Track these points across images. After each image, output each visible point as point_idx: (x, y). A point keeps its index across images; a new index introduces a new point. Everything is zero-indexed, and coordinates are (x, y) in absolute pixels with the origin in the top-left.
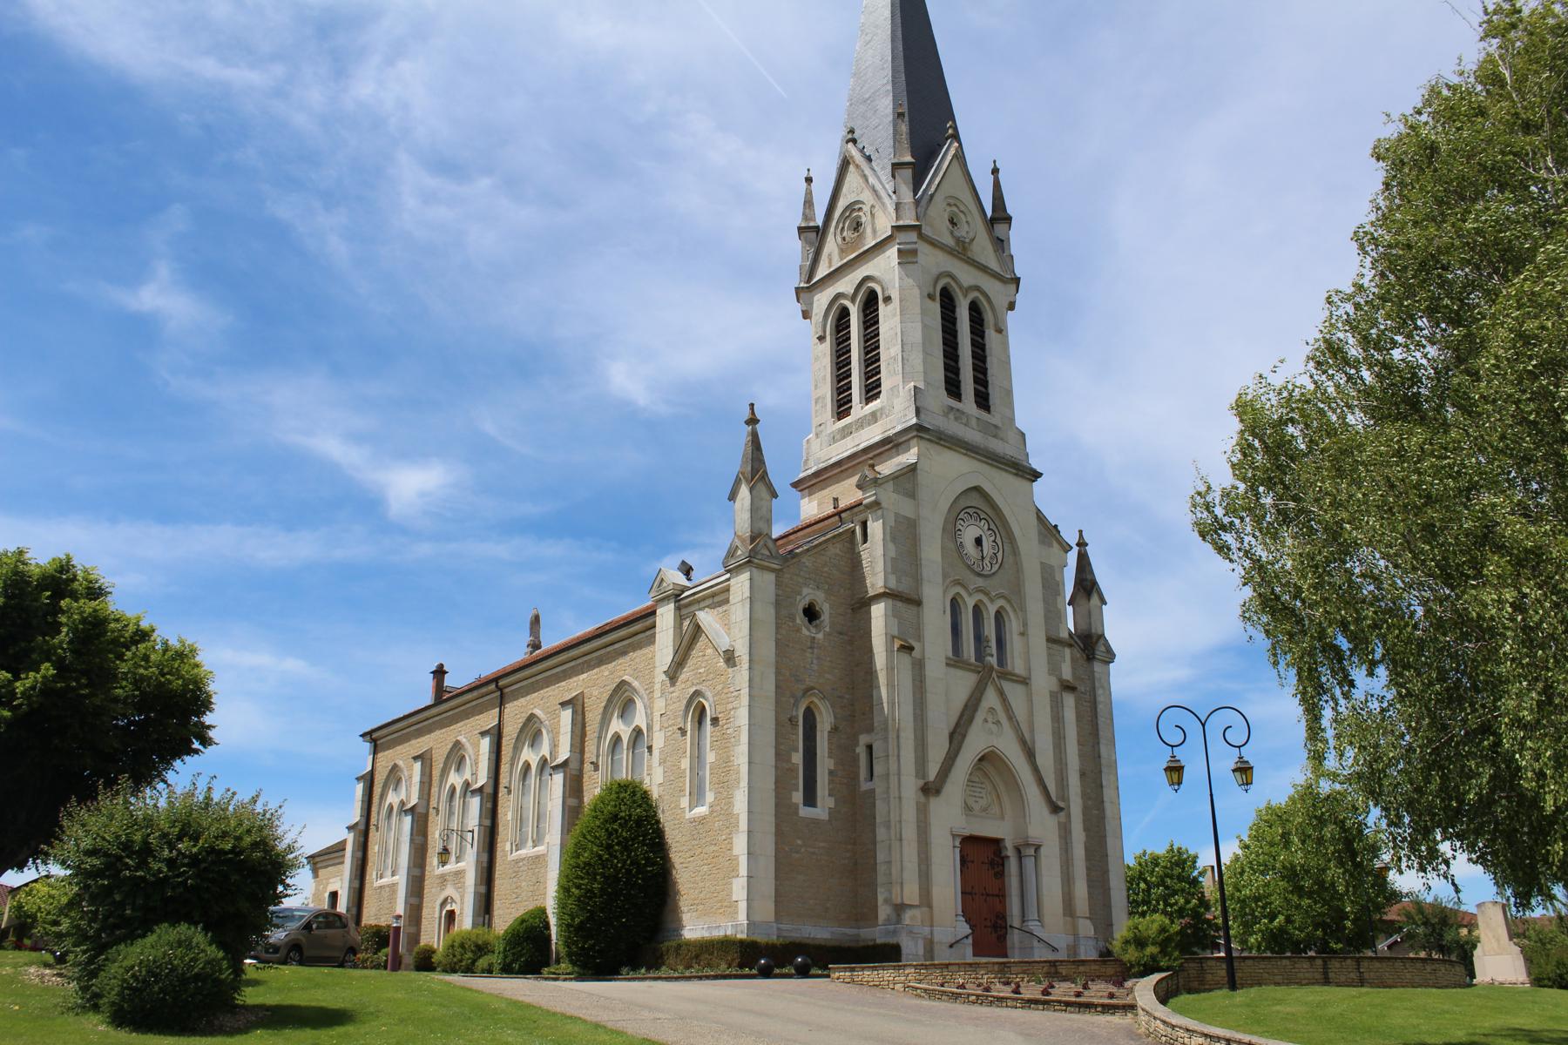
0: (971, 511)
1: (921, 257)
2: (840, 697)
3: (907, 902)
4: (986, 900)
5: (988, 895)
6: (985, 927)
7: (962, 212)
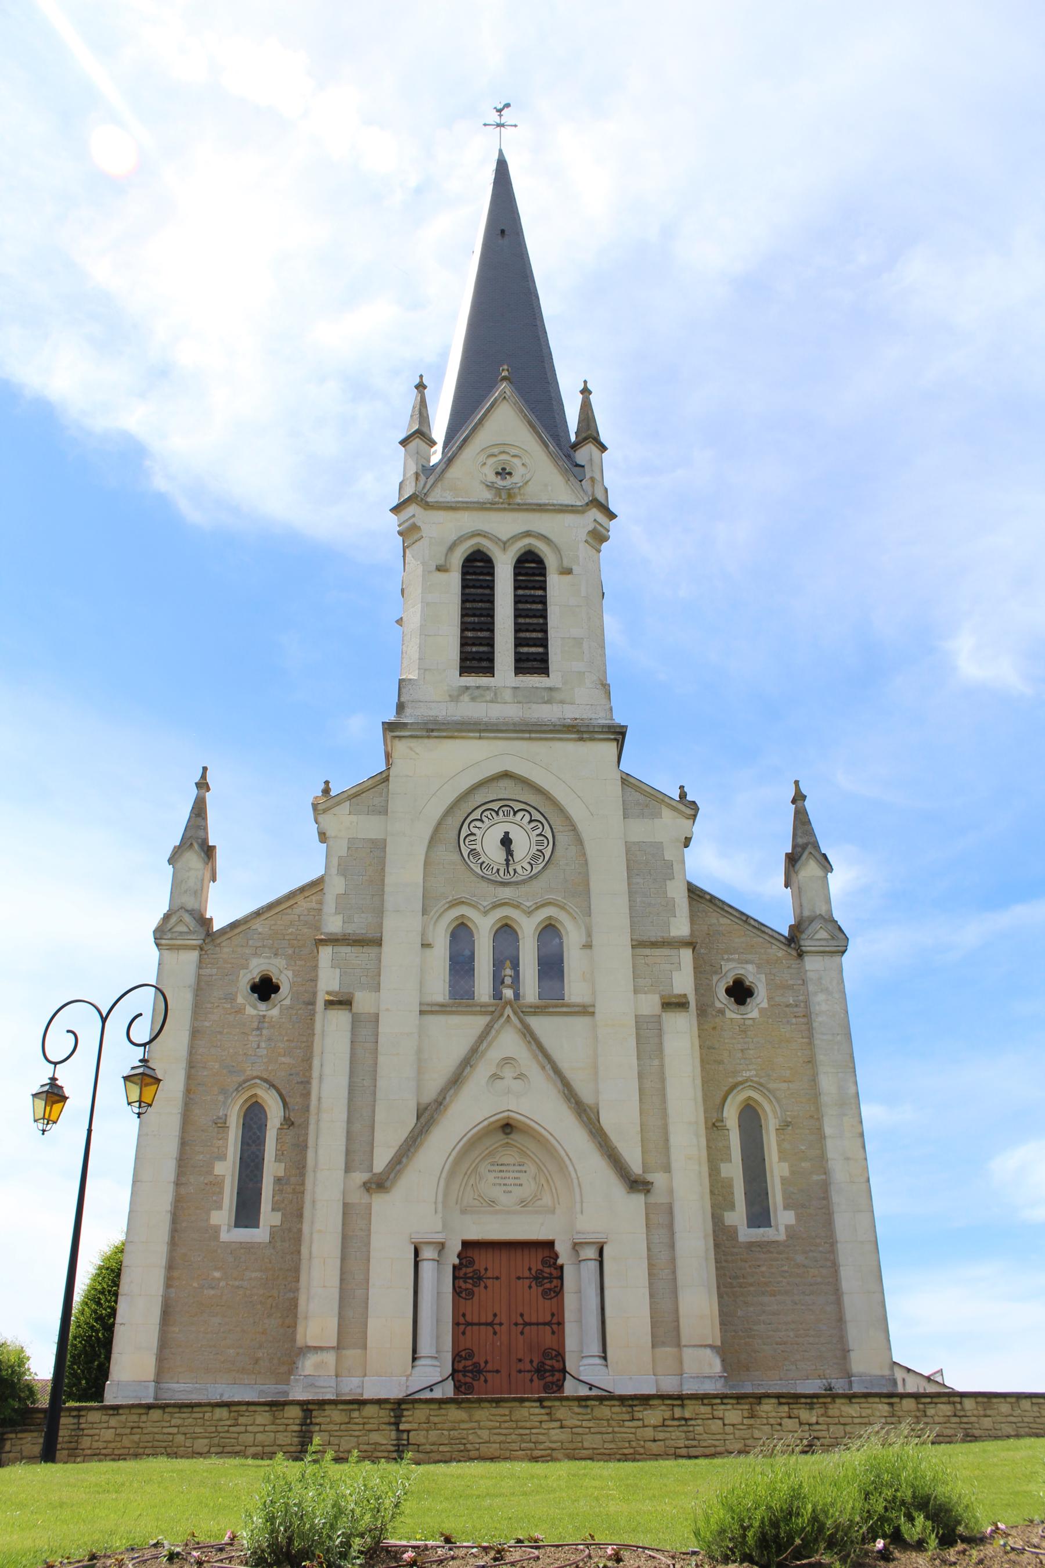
0: (495, 806)
1: (427, 530)
2: (302, 1082)
3: (311, 1343)
4: (522, 1333)
5: (526, 1324)
6: (520, 1371)
7: (514, 456)
